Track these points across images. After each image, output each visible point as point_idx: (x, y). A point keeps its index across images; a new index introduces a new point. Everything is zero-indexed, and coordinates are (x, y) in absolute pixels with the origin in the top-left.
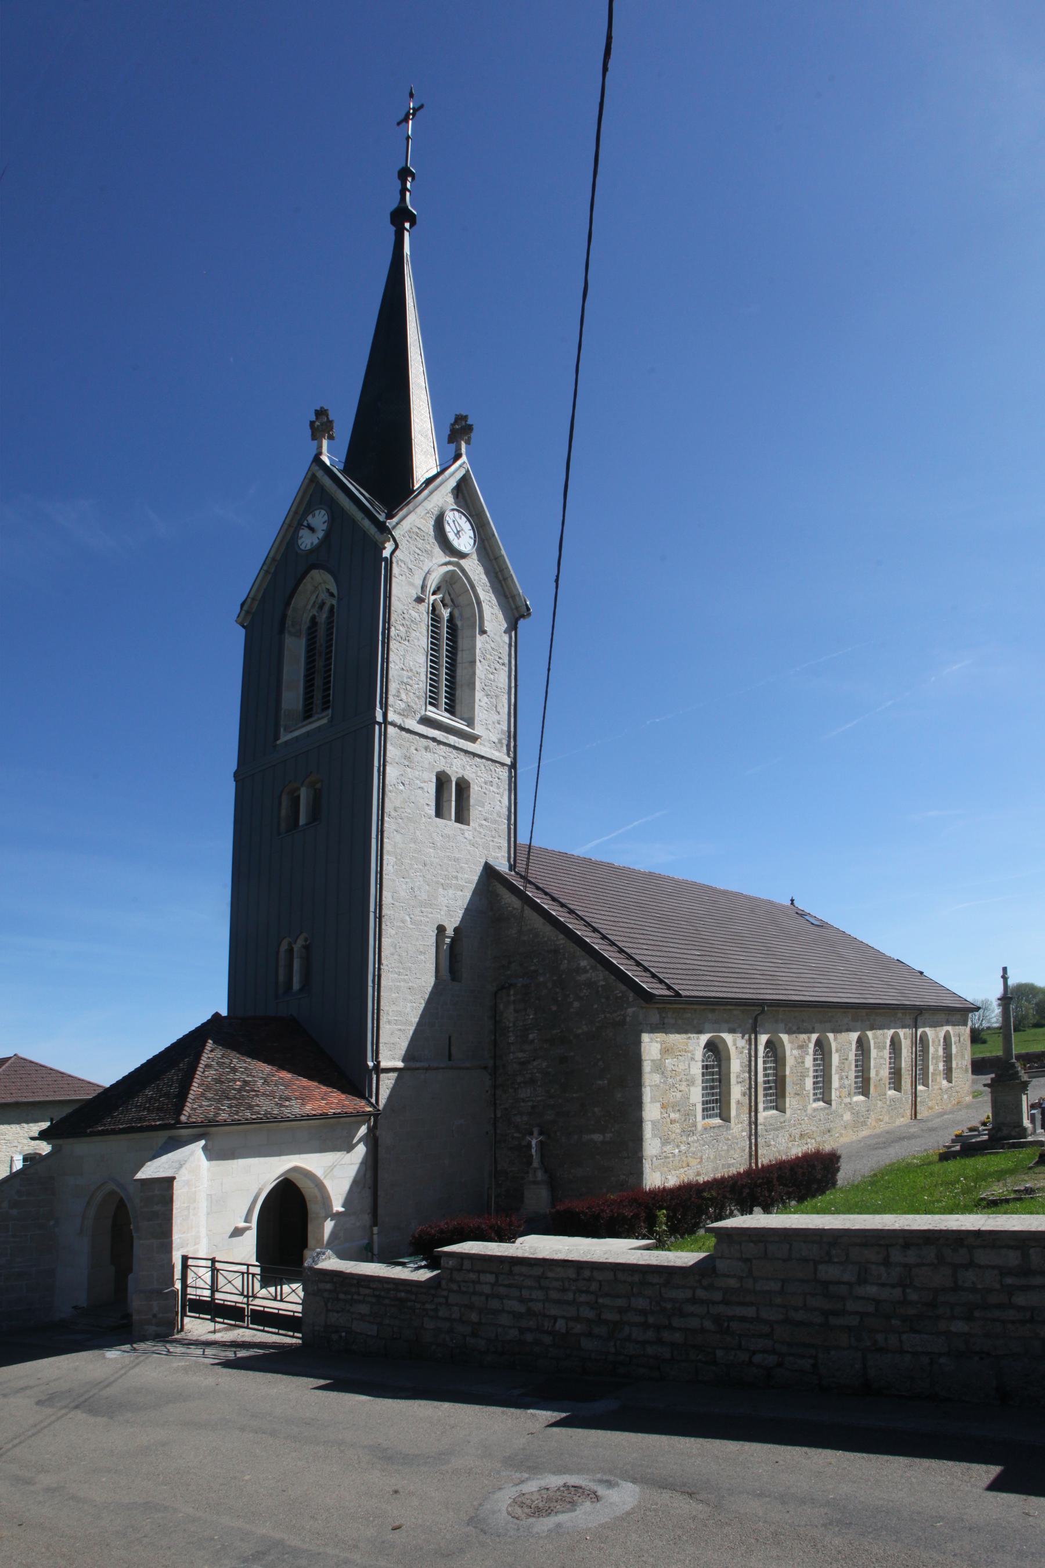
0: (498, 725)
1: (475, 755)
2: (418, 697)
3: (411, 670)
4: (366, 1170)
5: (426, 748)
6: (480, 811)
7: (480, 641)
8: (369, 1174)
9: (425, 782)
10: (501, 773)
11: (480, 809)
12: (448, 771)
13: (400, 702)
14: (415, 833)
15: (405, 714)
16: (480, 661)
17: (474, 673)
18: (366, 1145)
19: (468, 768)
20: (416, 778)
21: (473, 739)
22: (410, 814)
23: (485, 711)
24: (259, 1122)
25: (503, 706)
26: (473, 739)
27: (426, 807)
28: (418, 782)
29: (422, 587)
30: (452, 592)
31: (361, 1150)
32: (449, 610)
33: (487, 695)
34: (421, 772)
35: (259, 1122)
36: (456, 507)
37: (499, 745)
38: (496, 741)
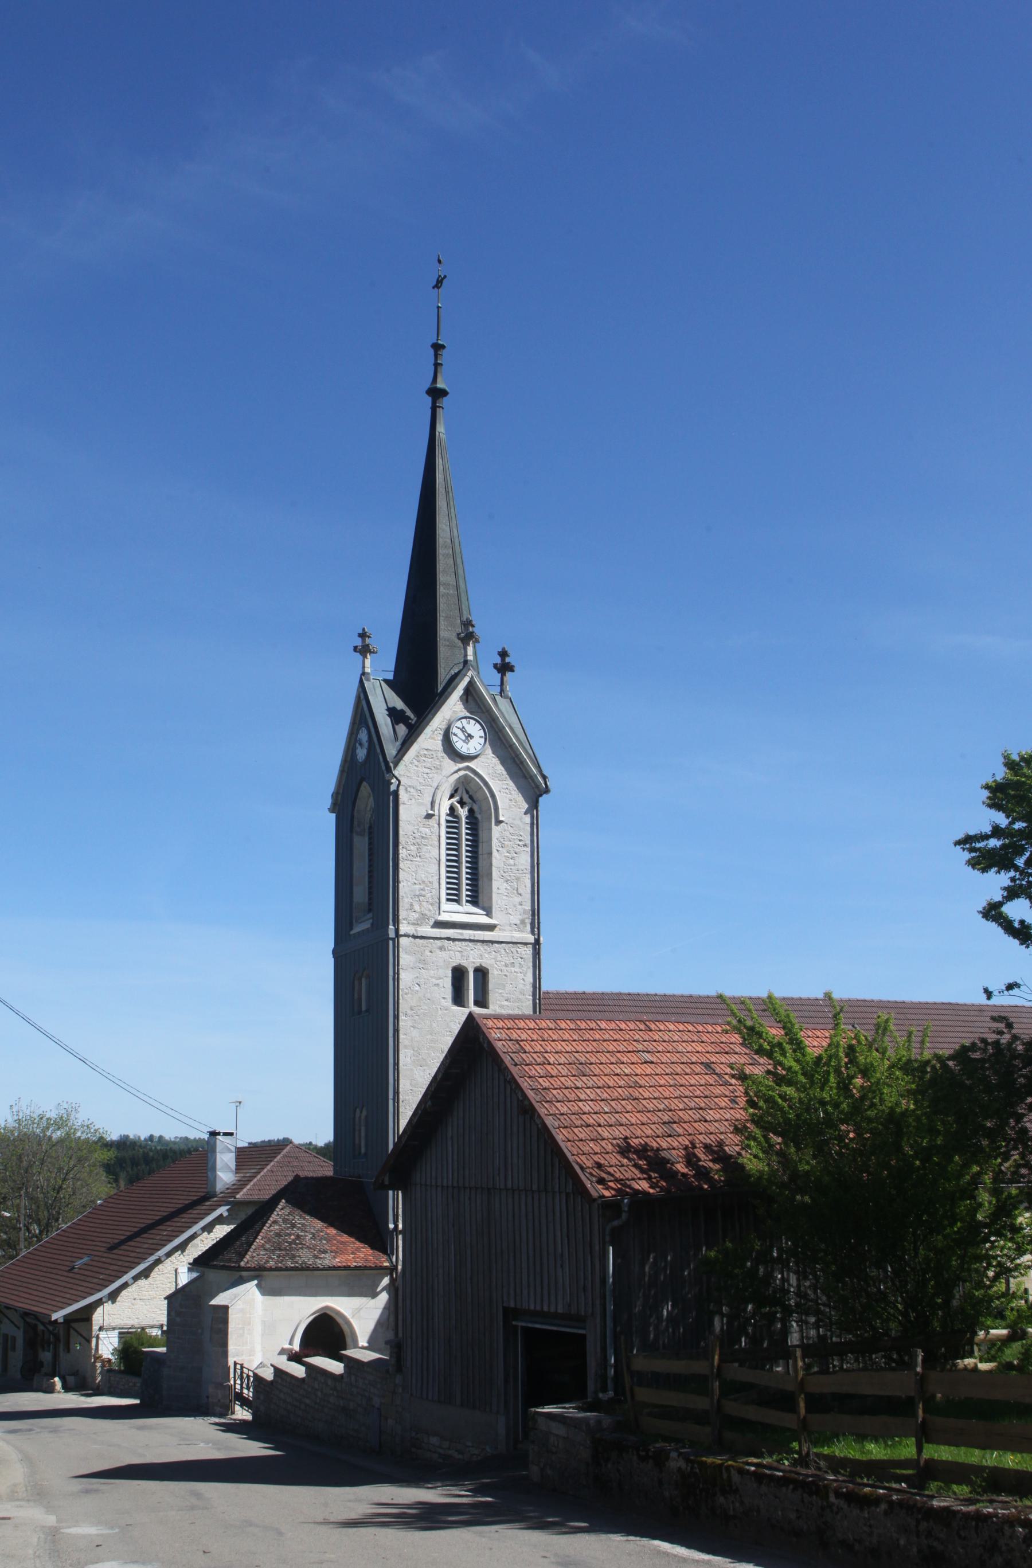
0: (520, 907)
1: (492, 942)
2: (432, 904)
3: (424, 882)
4: (389, 1315)
5: (441, 948)
6: (501, 994)
7: (496, 831)
8: (392, 1319)
9: (440, 978)
10: (524, 953)
11: (500, 991)
12: (464, 963)
13: (413, 914)
14: (431, 1025)
15: (419, 922)
16: (498, 851)
17: (491, 865)
18: (389, 1293)
19: (487, 956)
20: (432, 977)
21: (491, 928)
22: (425, 1010)
23: (504, 897)
24: (302, 1269)
25: (525, 886)
26: (491, 928)
27: (443, 1000)
28: (434, 980)
29: (433, 803)
30: (468, 788)
31: (384, 1297)
32: (466, 809)
33: (507, 881)
34: (436, 972)
35: (302, 1269)
36: (468, 715)
37: (521, 926)
38: (518, 922)
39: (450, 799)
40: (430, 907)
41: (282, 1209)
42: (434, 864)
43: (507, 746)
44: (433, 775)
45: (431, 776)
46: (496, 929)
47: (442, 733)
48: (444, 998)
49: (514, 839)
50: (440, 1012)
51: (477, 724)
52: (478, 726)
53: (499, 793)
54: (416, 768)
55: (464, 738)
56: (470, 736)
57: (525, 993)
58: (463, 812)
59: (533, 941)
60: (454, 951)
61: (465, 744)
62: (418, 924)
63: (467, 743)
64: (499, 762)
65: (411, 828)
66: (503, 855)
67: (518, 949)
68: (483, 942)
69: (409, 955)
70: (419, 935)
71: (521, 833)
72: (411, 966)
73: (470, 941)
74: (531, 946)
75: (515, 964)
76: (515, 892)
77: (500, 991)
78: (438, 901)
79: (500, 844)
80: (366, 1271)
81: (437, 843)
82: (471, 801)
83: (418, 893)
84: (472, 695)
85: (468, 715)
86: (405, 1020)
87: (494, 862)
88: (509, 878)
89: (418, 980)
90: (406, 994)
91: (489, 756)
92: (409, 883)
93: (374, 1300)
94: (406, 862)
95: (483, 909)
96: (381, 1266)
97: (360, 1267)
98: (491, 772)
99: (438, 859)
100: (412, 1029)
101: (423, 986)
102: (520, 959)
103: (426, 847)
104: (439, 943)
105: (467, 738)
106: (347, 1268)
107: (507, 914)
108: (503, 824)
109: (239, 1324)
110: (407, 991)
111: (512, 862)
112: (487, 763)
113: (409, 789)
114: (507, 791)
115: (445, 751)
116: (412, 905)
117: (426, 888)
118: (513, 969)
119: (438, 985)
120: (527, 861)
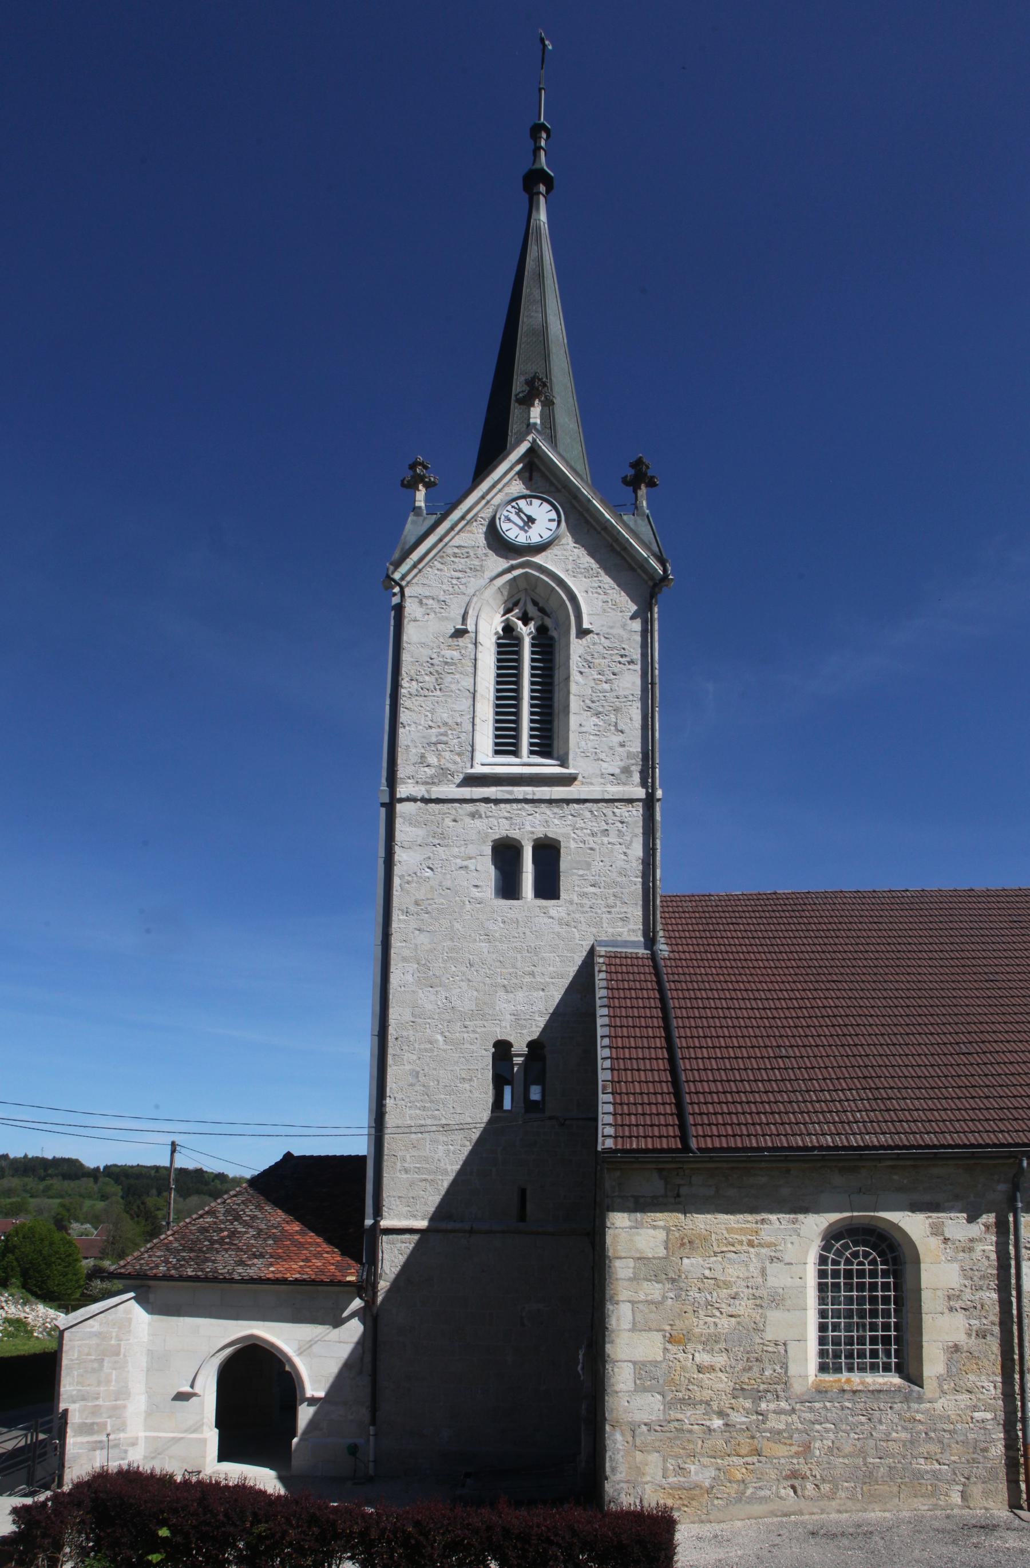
0: (621, 749)
1: (568, 802)
2: (459, 754)
3: (446, 724)
4: (364, 1352)
5: (473, 815)
6: (582, 876)
7: (577, 647)
8: (368, 1358)
9: (470, 858)
10: (627, 814)
11: (581, 872)
12: (515, 834)
13: (426, 769)
14: (452, 926)
15: (436, 780)
16: (581, 673)
17: (568, 693)
18: (363, 1321)
19: (556, 822)
20: (455, 857)
21: (568, 780)
22: (442, 904)
23: (592, 737)
24: (206, 1279)
25: (631, 719)
26: (568, 780)
27: (475, 890)
28: (458, 861)
29: (464, 618)
30: (537, 599)
31: (354, 1329)
32: (532, 626)
33: (598, 714)
34: (463, 849)
35: (215, 1280)
36: (528, 492)
37: (623, 777)
38: (617, 771)
39: (504, 615)
40: (457, 759)
41: (235, 1196)
42: (466, 698)
43: (599, 529)
44: (469, 579)
45: (463, 581)
46: (576, 783)
47: (486, 523)
48: (476, 886)
49: (611, 655)
50: (468, 907)
51: (545, 504)
52: (546, 507)
53: (584, 594)
54: (439, 573)
55: (521, 524)
56: (531, 520)
57: (629, 873)
58: (526, 632)
59: (644, 796)
60: (497, 818)
61: (522, 533)
62: (433, 783)
63: (526, 532)
64: (585, 553)
65: (424, 653)
66: (591, 678)
67: (616, 810)
68: (550, 802)
69: (415, 826)
70: (433, 797)
71: (624, 646)
72: (419, 843)
73: (526, 801)
74: (640, 804)
75: (610, 832)
76: (613, 728)
77: (581, 872)
78: (470, 749)
79: (585, 664)
80: (320, 1288)
81: (471, 670)
82: (540, 614)
83: (434, 739)
84: (539, 470)
85: (528, 492)
86: (405, 920)
87: (574, 688)
88: (601, 710)
89: (430, 862)
90: (408, 883)
91: (568, 547)
92: (421, 727)
93: (337, 1330)
94: (417, 698)
95: (557, 759)
96: (340, 1281)
97: (304, 1280)
98: (570, 567)
99: (472, 690)
100: (417, 932)
101: (439, 870)
102: (620, 825)
103: (452, 676)
104: (469, 808)
105: (526, 524)
106: (284, 1281)
107: (598, 759)
108: (591, 635)
109: (88, 1354)
110: (410, 879)
111: (607, 687)
112: (563, 555)
113: (425, 601)
114: (599, 590)
115: (490, 546)
116: (423, 756)
117: (450, 732)
118: (605, 840)
119: (466, 867)
120: (634, 683)
